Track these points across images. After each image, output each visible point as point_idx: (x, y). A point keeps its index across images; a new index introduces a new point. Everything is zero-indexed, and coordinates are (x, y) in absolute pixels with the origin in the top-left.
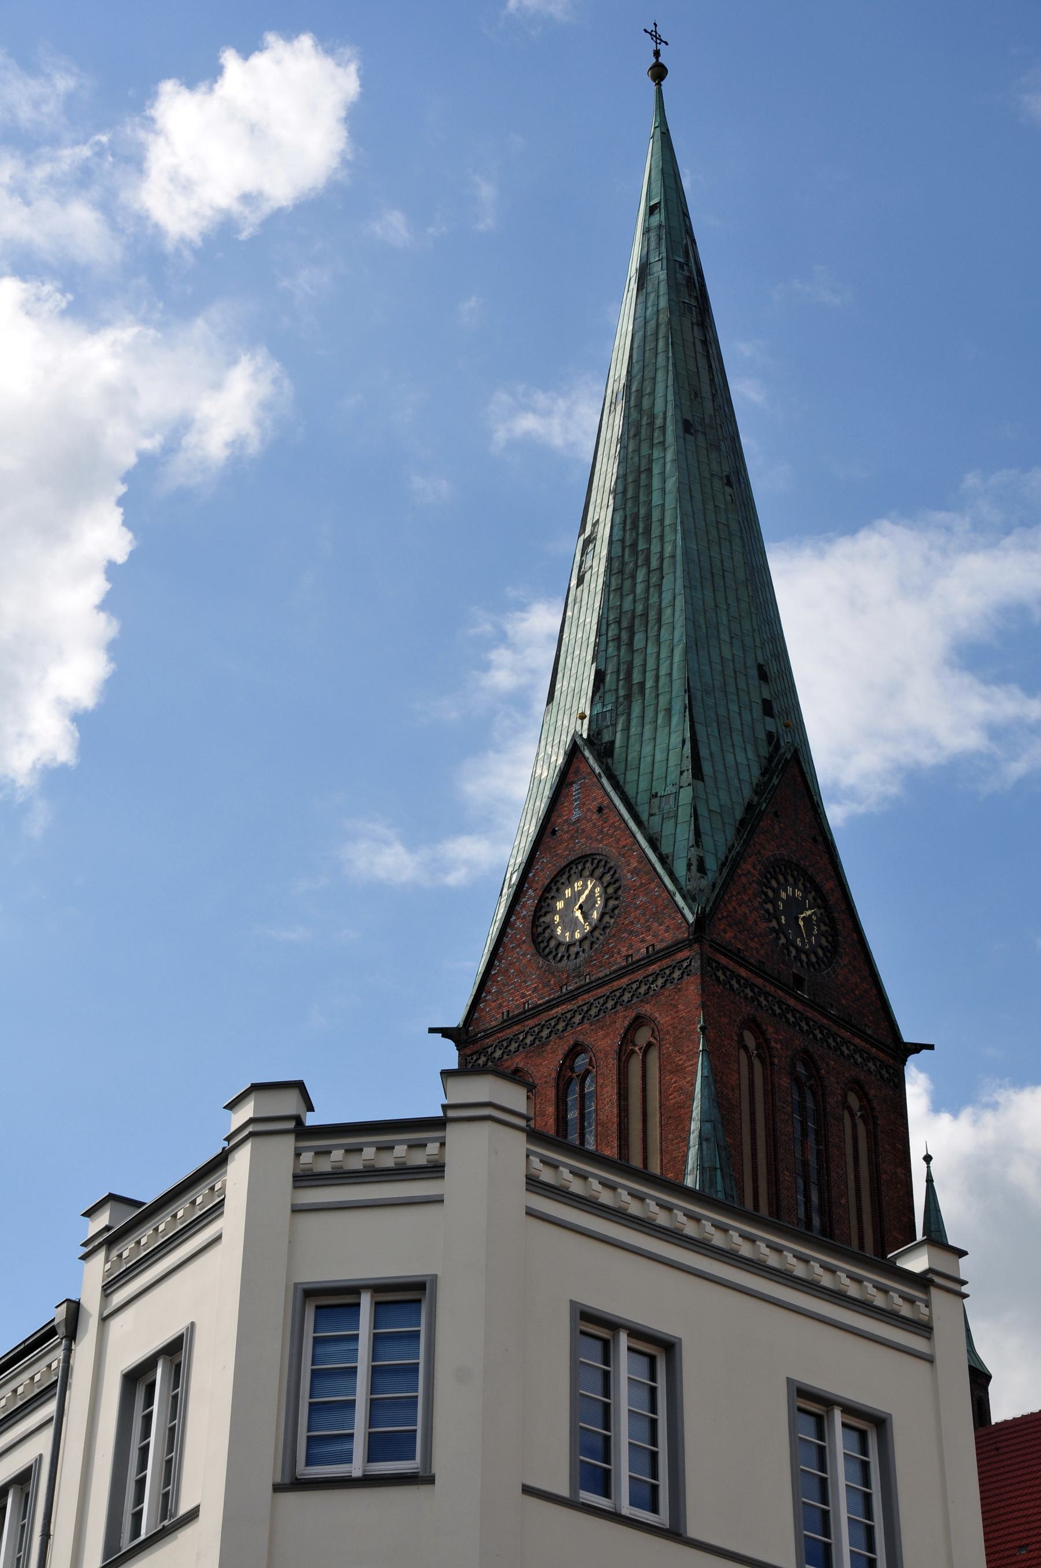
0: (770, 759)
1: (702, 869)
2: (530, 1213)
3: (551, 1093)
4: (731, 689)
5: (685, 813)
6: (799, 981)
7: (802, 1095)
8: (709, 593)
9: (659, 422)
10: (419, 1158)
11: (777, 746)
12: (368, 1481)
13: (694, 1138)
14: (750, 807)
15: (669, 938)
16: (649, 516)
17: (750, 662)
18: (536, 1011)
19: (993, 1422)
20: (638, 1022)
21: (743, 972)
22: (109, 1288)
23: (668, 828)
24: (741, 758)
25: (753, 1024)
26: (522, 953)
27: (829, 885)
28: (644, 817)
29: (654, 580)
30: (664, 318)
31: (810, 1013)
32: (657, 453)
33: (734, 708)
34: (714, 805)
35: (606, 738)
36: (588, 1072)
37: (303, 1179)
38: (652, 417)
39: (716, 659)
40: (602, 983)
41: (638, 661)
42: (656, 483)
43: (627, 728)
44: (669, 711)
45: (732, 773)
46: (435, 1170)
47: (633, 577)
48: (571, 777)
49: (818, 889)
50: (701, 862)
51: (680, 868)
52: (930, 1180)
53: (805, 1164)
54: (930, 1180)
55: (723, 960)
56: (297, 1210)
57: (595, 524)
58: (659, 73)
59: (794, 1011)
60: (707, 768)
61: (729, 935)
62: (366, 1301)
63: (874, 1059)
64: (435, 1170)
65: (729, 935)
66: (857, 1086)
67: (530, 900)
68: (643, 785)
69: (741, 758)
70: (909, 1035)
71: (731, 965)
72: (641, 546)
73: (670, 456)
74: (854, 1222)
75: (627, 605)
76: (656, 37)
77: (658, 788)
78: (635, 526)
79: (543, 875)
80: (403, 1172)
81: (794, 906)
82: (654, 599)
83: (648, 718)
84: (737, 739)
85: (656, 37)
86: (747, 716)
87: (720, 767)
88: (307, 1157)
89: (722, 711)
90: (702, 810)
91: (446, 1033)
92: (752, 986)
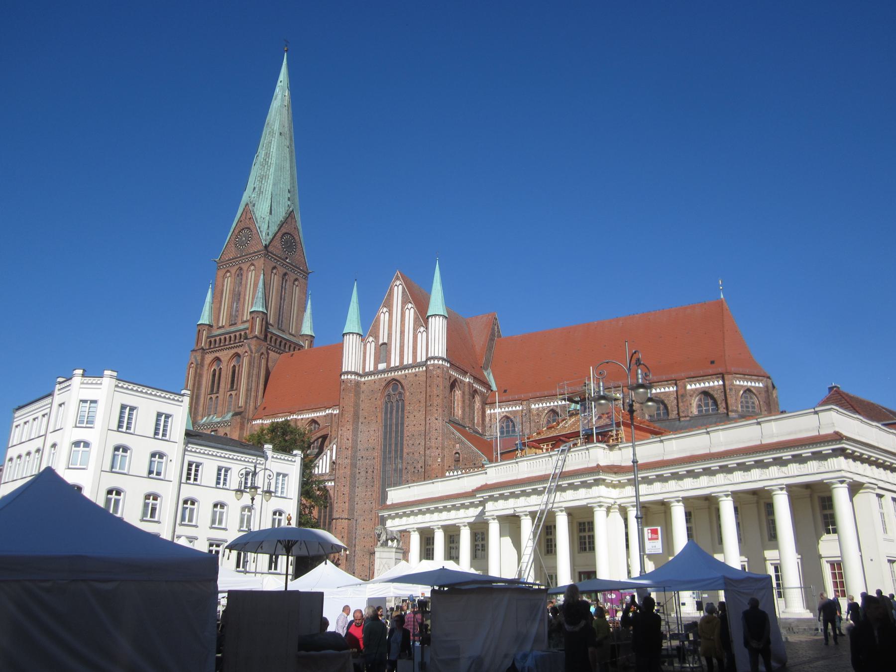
5: (267, 222)
8: (280, 172)
9: (275, 132)
16: (269, 153)
17: (286, 188)
24: (281, 210)
31: (288, 265)
32: (273, 139)
34: (273, 221)
38: (273, 130)
39: (279, 188)
42: (272, 146)
44: (267, 198)
45: (278, 213)
47: (264, 167)
50: (268, 233)
51: (264, 234)
60: (273, 212)
61: (272, 249)
64: (101, 384)
65: (272, 249)
69: (281, 210)
72: (267, 160)
73: (276, 140)
77: (263, 217)
78: (266, 154)
82: (268, 173)
83: (263, 199)
86: (284, 201)
89: (278, 200)
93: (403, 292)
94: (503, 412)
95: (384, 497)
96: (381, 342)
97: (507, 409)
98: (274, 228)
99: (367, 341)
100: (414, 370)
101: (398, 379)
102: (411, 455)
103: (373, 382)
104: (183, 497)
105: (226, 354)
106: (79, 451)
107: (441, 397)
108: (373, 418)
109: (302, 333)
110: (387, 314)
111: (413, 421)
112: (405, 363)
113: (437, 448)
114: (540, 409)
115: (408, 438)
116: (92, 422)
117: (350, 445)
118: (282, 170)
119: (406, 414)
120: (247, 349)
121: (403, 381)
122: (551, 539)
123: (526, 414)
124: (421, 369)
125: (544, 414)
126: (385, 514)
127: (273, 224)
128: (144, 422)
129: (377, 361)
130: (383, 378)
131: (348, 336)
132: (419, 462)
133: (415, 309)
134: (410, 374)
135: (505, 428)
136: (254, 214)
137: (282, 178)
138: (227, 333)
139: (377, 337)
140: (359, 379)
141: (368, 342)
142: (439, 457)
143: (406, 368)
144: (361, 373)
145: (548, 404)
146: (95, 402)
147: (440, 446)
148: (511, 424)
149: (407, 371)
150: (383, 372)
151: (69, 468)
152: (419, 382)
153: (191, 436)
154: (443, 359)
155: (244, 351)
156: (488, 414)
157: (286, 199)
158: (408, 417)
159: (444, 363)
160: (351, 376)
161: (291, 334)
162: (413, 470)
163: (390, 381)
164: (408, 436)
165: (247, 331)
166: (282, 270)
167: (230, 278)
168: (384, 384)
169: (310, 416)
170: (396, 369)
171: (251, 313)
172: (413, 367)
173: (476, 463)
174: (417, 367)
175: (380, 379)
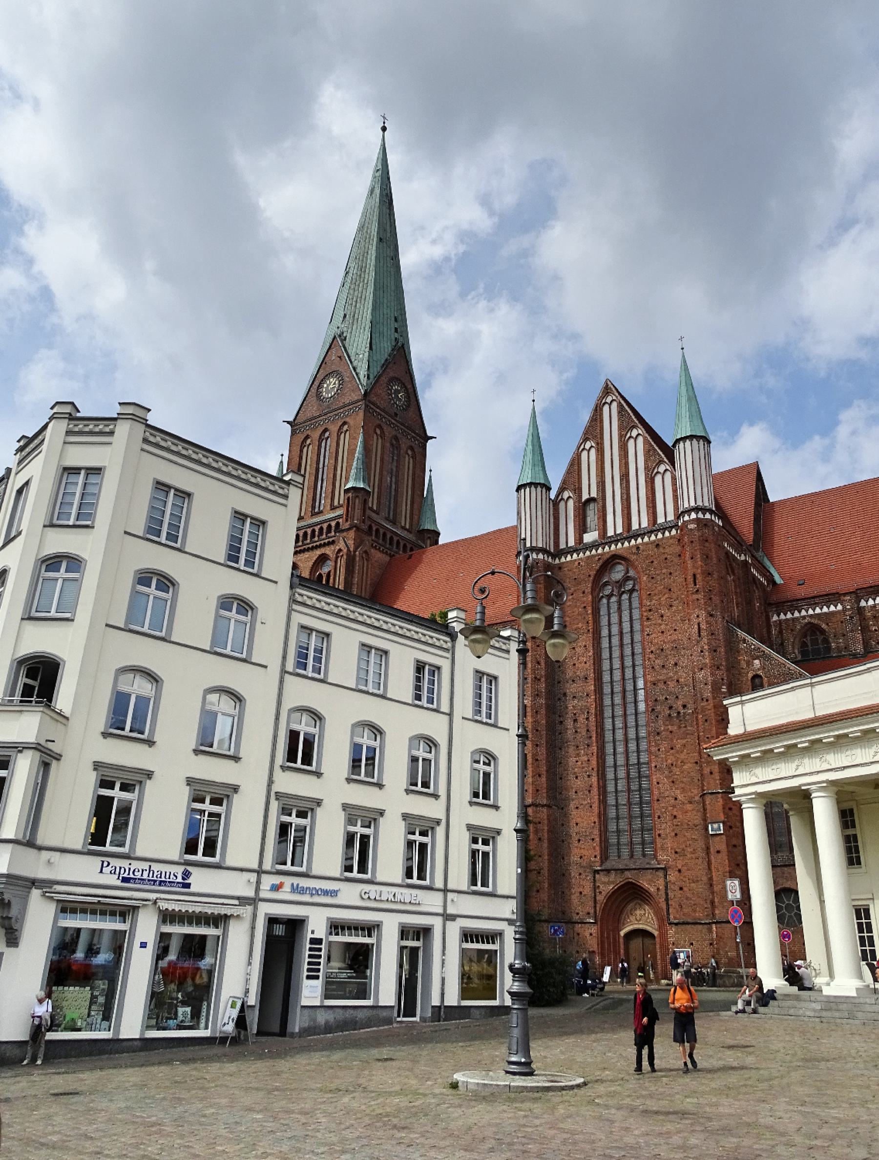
0: (395, 346)
1: (368, 378)
2: (142, 450)
4: (385, 323)
6: (396, 414)
7: (393, 449)
10: (107, 430)
11: (398, 342)
14: (386, 360)
15: (356, 398)
17: (392, 315)
18: (315, 418)
20: (345, 423)
21: (378, 410)
25: (380, 427)
26: (313, 399)
27: (409, 386)
28: (353, 360)
33: (385, 329)
35: (344, 335)
36: (328, 437)
37: (69, 433)
40: (335, 410)
41: (357, 312)
45: (382, 350)
46: (112, 433)
48: (333, 346)
49: (406, 387)
51: (361, 377)
52: (430, 477)
53: (392, 469)
54: (430, 477)
55: (372, 406)
56: (65, 443)
59: (393, 424)
60: (374, 347)
61: (375, 399)
66: (411, 448)
67: (317, 383)
68: (354, 350)
70: (429, 434)
71: (374, 408)
74: (405, 487)
79: (320, 376)
80: (101, 433)
81: (397, 392)
84: (385, 339)
87: (378, 347)
88: (71, 426)
89: (381, 330)
90: (370, 360)
91: (288, 422)
92: (381, 415)
94: (804, 617)
95: (723, 720)
96: (585, 496)
97: (811, 612)
98: (376, 370)
99: (560, 497)
100: (653, 538)
101: (625, 555)
103: (576, 563)
104: (288, 704)
105: (308, 558)
106: (57, 579)
107: (715, 576)
108: (580, 625)
110: (593, 451)
112: (635, 526)
113: (718, 668)
116: (91, 516)
117: (543, 673)
118: (385, 289)
119: (645, 614)
121: (634, 557)
123: (852, 618)
124: (667, 534)
126: (732, 755)
127: (375, 364)
129: (582, 528)
130: (594, 556)
131: (528, 489)
132: (680, 697)
134: (647, 544)
135: (809, 644)
136: (346, 350)
137: (385, 301)
138: (309, 526)
139: (578, 490)
140: (550, 560)
141: (562, 499)
142: (723, 684)
143: (639, 535)
144: (552, 551)
147: (724, 663)
148: (820, 638)
149: (639, 540)
150: (594, 545)
152: (666, 556)
155: (338, 548)
156: (775, 621)
157: (393, 330)
158: (648, 619)
159: (713, 518)
160: (537, 554)
161: (404, 528)
163: (608, 559)
164: (652, 652)
165: (341, 520)
166: (389, 432)
167: (311, 446)
168: (596, 566)
170: (617, 539)
172: (651, 532)
174: (658, 530)
175: (588, 557)
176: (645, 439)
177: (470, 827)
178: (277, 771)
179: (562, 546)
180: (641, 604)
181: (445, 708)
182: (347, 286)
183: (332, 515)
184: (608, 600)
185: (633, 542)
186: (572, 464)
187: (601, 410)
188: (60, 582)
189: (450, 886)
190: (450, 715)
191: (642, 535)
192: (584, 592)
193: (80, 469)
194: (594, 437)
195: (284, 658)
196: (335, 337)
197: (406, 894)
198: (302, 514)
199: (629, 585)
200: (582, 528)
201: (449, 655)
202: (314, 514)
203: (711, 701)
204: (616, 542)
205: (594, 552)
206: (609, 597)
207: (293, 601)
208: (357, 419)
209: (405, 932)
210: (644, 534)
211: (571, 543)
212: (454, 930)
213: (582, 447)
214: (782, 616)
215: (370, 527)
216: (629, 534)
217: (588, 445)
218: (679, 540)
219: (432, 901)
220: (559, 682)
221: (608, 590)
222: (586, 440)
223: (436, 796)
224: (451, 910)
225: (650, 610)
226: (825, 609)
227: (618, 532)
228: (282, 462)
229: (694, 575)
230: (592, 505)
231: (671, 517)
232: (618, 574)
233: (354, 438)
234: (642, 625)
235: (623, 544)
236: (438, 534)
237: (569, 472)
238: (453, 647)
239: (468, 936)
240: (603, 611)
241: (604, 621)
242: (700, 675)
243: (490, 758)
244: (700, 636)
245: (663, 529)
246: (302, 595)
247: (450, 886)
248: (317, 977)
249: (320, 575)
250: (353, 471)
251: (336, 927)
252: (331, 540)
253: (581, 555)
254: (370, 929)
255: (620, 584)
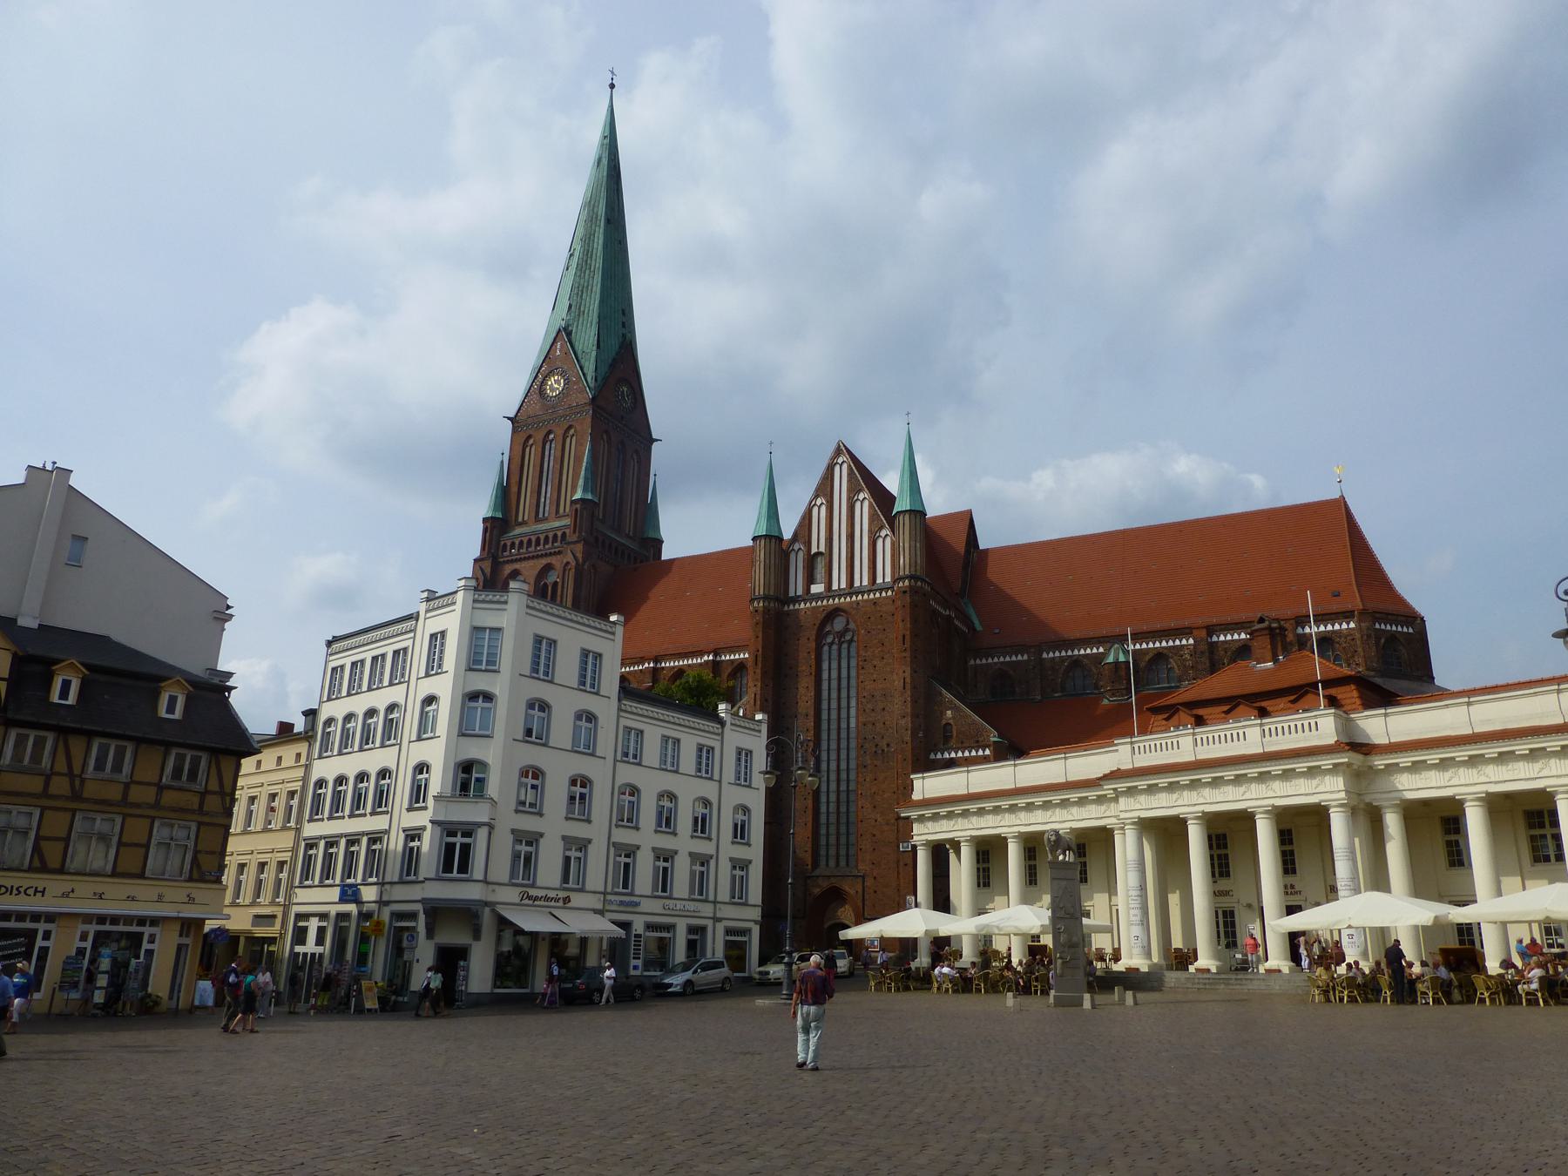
1: (596, 380)
2: (527, 613)
3: (541, 445)
6: (622, 418)
9: (599, 218)
12: (486, 671)
13: (584, 468)
14: (614, 359)
19: (665, 557)
22: (427, 611)
23: (587, 364)
25: (606, 432)
26: (536, 397)
28: (580, 358)
29: (591, 275)
30: (605, 179)
35: (570, 328)
37: (475, 601)
43: (577, 327)
47: (585, 273)
49: (632, 388)
51: (589, 379)
52: (655, 481)
54: (655, 481)
57: (574, 249)
58: (612, 86)
60: (601, 344)
62: (488, 631)
63: (641, 443)
64: (506, 602)
66: (637, 452)
68: (581, 346)
73: (602, 230)
75: (582, 283)
76: (612, 72)
78: (587, 255)
82: (591, 282)
85: (612, 72)
88: (476, 596)
91: (509, 418)
93: (849, 474)
96: (814, 550)
97: (1002, 659)
100: (872, 596)
102: (870, 726)
104: (620, 781)
106: (477, 708)
109: (645, 536)
110: (823, 509)
111: (872, 674)
112: (857, 584)
114: (1057, 660)
115: (863, 700)
119: (861, 663)
120: (570, 558)
122: (1457, 842)
123: (1035, 667)
124: (884, 594)
125: (1063, 668)
128: (567, 666)
130: (819, 607)
133: (872, 500)
134: (866, 601)
138: (534, 533)
141: (793, 550)
144: (782, 597)
145: (1070, 653)
146: (499, 630)
149: (860, 597)
150: (819, 597)
151: (464, 735)
153: (627, 689)
154: (923, 580)
155: (565, 561)
157: (620, 326)
161: (628, 536)
162: (874, 749)
165: (567, 531)
169: (676, 664)
171: (573, 502)
173: (980, 739)
174: (877, 590)
176: (870, 502)
177: (731, 859)
178: (613, 827)
179: (792, 594)
180: (858, 653)
181: (716, 777)
182: (573, 270)
183: (557, 524)
184: (830, 647)
185: (854, 598)
186: (803, 518)
187: (833, 470)
188: (479, 709)
189: (719, 899)
190: (720, 781)
191: (863, 593)
192: (808, 639)
193: (485, 628)
194: (825, 496)
195: (616, 751)
196: (560, 330)
197: (691, 906)
198: (526, 518)
199: (848, 637)
200: (810, 580)
201: (719, 738)
202: (537, 520)
203: (909, 744)
204: (840, 596)
205: (819, 603)
206: (831, 644)
207: (620, 709)
208: (585, 425)
209: (692, 930)
210: (864, 592)
211: (800, 592)
212: (720, 928)
213: (813, 503)
214: (978, 661)
215: (597, 539)
216: (851, 589)
217: (819, 501)
218: (894, 601)
219: (707, 910)
220: (783, 717)
221: (829, 640)
222: (816, 496)
223: (709, 839)
224: (718, 915)
225: (865, 660)
226: (1014, 658)
227: (841, 587)
228: (502, 462)
229: (904, 636)
230: (819, 559)
231: (888, 579)
232: (839, 624)
233: (580, 444)
234: (858, 673)
235: (845, 599)
236: (659, 542)
237: (801, 525)
238: (723, 732)
239: (729, 931)
240: (825, 656)
241: (825, 666)
242: (903, 722)
243: (746, 810)
244: (904, 688)
245: (881, 590)
246: (625, 705)
247: (719, 899)
248: (639, 958)
249: (545, 584)
250: (581, 482)
251: (650, 927)
252: (557, 550)
253: (808, 604)
254: (670, 928)
255: (841, 634)
